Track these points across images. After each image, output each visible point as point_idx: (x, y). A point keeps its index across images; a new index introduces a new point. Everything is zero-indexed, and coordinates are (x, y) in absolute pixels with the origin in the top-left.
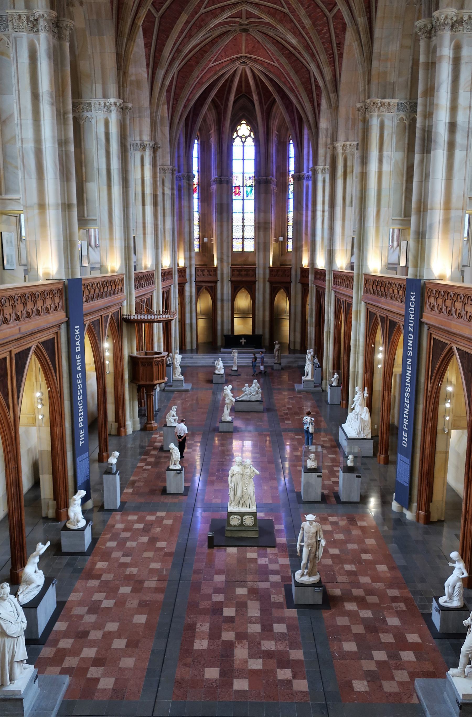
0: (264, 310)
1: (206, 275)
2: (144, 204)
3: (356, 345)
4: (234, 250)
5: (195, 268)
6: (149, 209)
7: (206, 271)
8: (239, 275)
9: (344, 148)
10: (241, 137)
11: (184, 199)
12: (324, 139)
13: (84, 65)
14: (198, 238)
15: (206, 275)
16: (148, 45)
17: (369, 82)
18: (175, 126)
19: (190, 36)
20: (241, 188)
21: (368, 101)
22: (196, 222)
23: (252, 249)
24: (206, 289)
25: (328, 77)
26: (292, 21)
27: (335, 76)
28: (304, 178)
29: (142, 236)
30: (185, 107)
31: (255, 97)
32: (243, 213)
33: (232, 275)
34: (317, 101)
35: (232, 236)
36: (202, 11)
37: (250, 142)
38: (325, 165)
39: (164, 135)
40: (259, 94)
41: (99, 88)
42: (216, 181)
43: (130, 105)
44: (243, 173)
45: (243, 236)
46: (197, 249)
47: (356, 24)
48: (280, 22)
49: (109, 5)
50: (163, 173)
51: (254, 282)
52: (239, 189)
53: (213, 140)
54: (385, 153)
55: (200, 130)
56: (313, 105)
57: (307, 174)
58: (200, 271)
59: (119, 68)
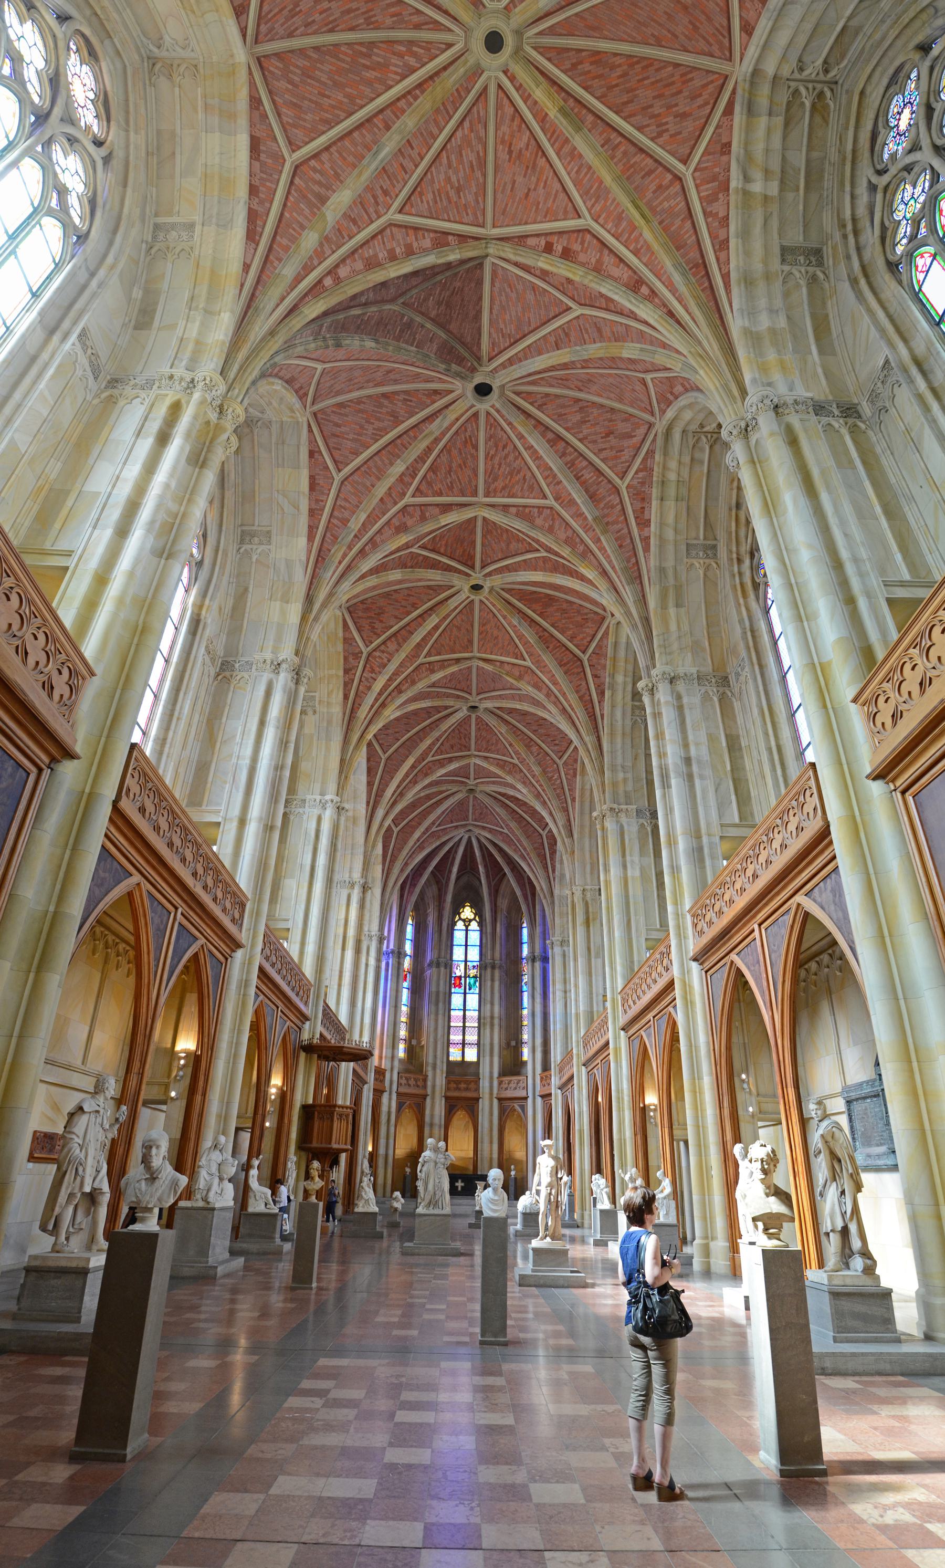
0: (491, 1142)
2: (343, 949)
4: (451, 1058)
6: (349, 954)
8: (458, 1089)
10: (464, 920)
13: (304, 766)
16: (370, 784)
17: (604, 792)
18: (389, 889)
19: (414, 782)
21: (604, 807)
22: (404, 1019)
23: (475, 1059)
24: (410, 1107)
25: (561, 822)
26: (521, 771)
27: (569, 821)
29: (336, 987)
30: (402, 870)
31: (481, 869)
32: (465, 1010)
33: (448, 1089)
35: (448, 1039)
36: (430, 759)
37: (474, 925)
40: (486, 866)
41: (317, 787)
42: (430, 965)
43: (346, 806)
44: (466, 961)
45: (464, 1040)
46: (401, 1054)
47: (585, 744)
48: (510, 773)
49: (341, 715)
51: (477, 1099)
53: (431, 919)
54: (628, 858)
55: (416, 908)
59: (341, 772)
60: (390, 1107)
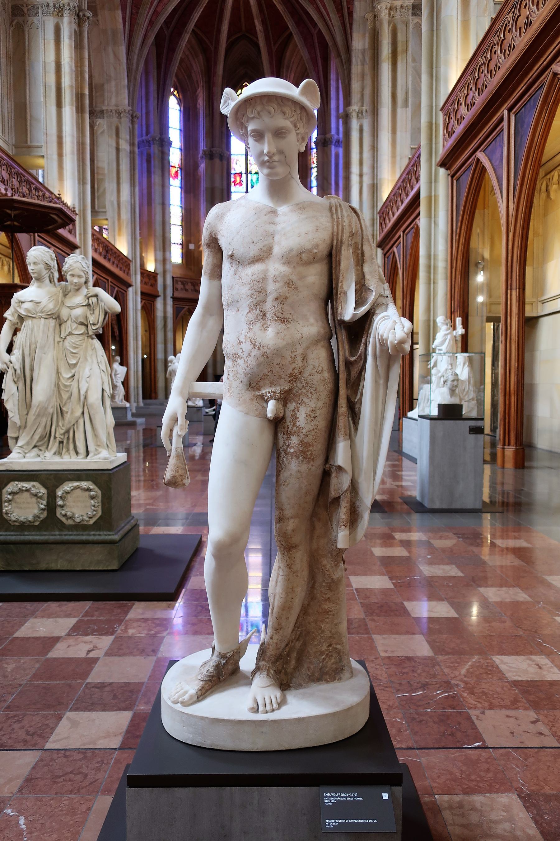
1: (190, 290)
2: (59, 105)
3: (429, 267)
5: (173, 278)
6: (68, 112)
7: (189, 284)
9: (392, 13)
11: (154, 172)
12: (360, 67)
14: (181, 244)
15: (190, 290)
20: (244, 176)
28: (331, 142)
29: (55, 157)
30: (152, 23)
31: (259, 26)
34: (348, 8)
38: (362, 106)
39: (119, 60)
40: (264, 22)
50: (118, 117)
52: (241, 177)
56: (342, 17)
57: (336, 137)
58: (180, 283)
60: (165, 312)
